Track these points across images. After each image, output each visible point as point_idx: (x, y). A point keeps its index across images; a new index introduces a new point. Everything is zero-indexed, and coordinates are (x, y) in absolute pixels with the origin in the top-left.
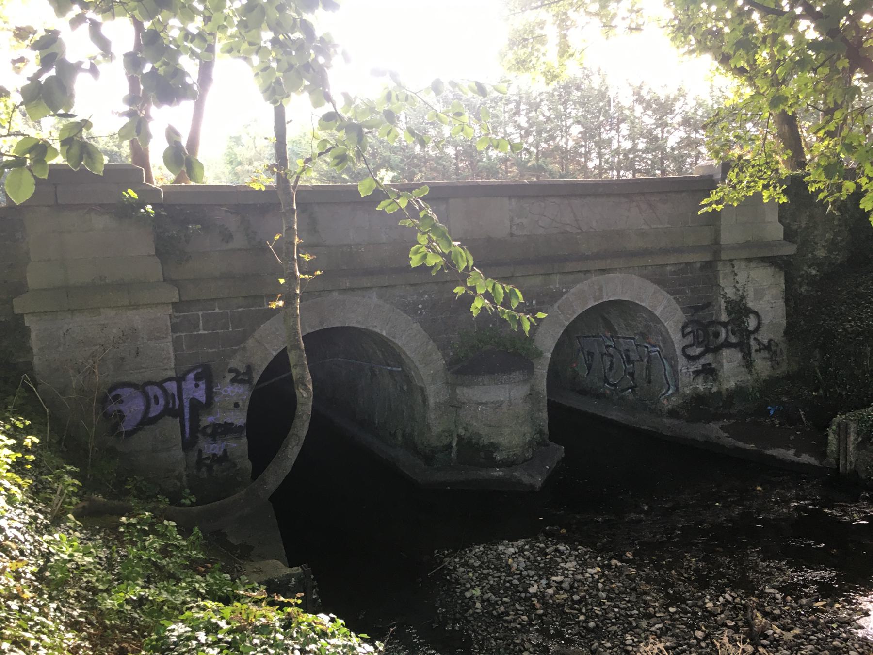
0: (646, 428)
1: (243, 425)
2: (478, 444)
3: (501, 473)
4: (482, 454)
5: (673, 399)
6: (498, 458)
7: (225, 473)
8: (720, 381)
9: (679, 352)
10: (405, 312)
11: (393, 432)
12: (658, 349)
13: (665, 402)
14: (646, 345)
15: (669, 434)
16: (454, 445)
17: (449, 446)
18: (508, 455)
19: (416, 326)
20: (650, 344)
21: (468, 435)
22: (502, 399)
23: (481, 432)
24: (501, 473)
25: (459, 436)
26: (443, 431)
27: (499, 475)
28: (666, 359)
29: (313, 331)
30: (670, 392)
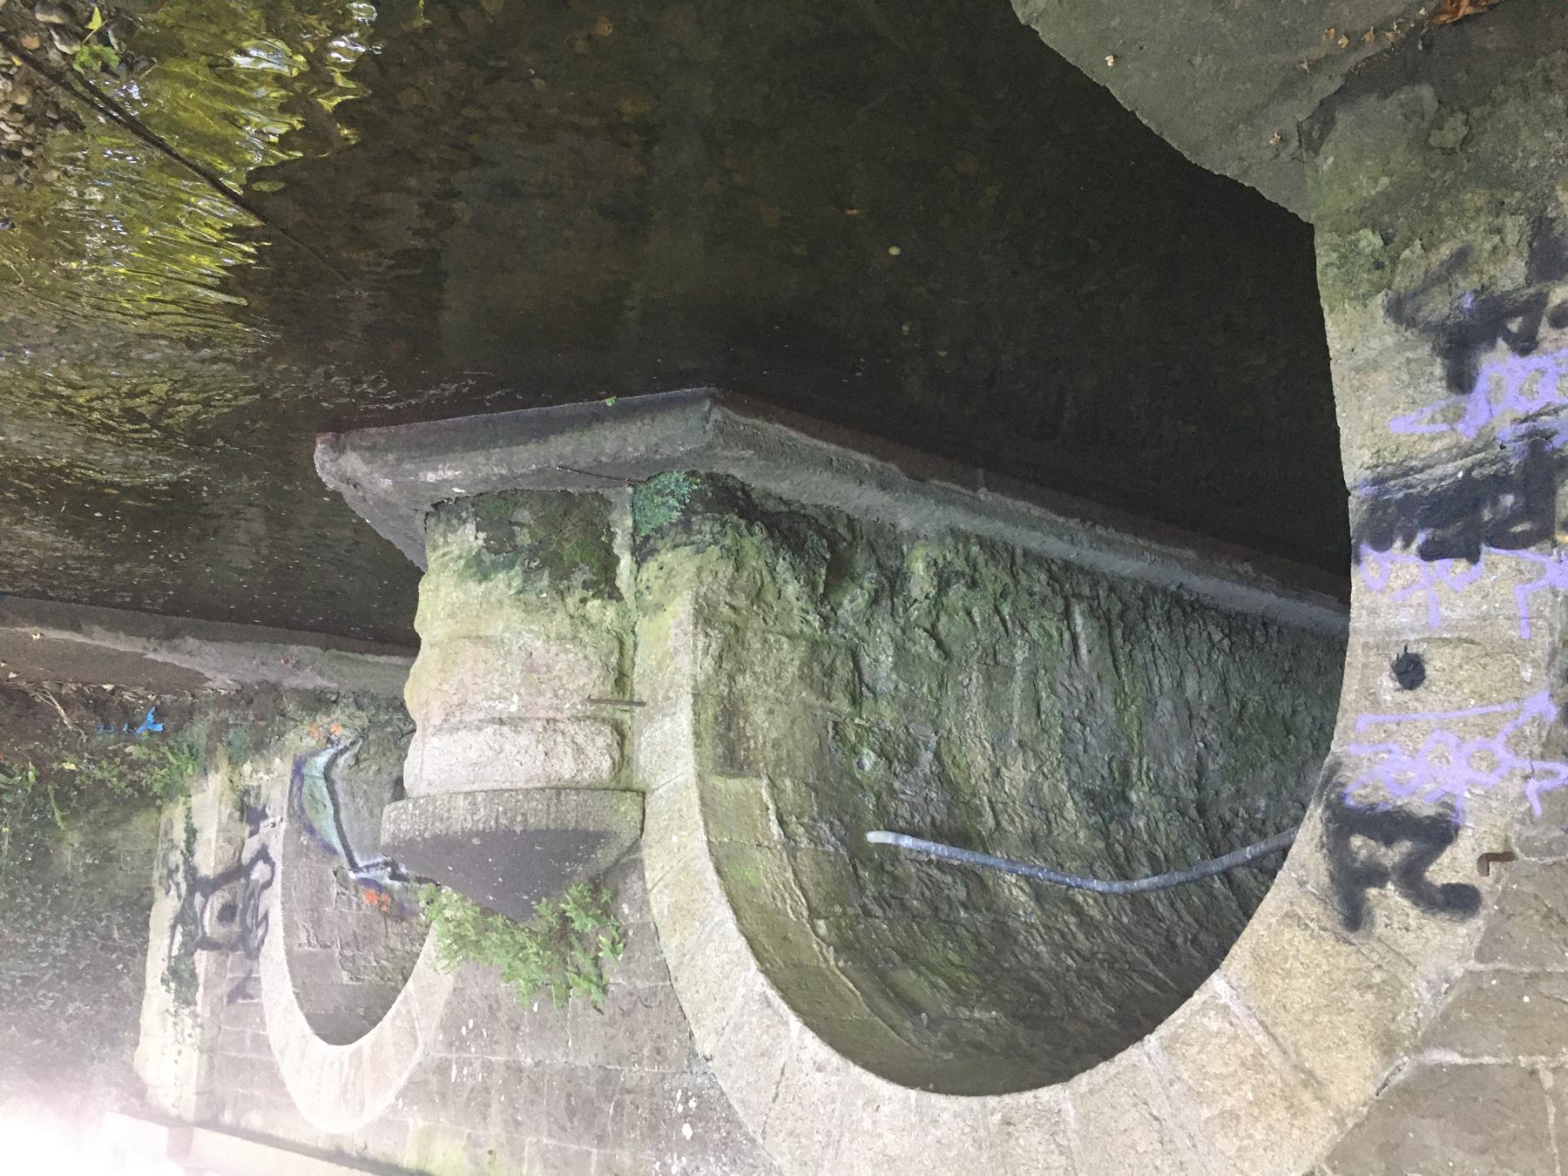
0: (383, 659)
1: (1369, 555)
2: (528, 574)
3: (431, 477)
4: (524, 538)
5: (309, 742)
6: (470, 528)
7: (1445, 251)
8: (233, 789)
9: (279, 868)
10: (731, 1120)
11: (957, 590)
12: (352, 876)
13: (338, 732)
14: (397, 884)
15: (295, 649)
16: (626, 562)
17: (642, 553)
18: (446, 543)
19: (705, 1046)
20: (381, 888)
21: (572, 601)
22: (435, 741)
23: (517, 615)
24: (431, 477)
25: (614, 595)
26: (660, 607)
27: (435, 470)
28: (331, 850)
29: (1046, 1094)
30: (322, 760)
